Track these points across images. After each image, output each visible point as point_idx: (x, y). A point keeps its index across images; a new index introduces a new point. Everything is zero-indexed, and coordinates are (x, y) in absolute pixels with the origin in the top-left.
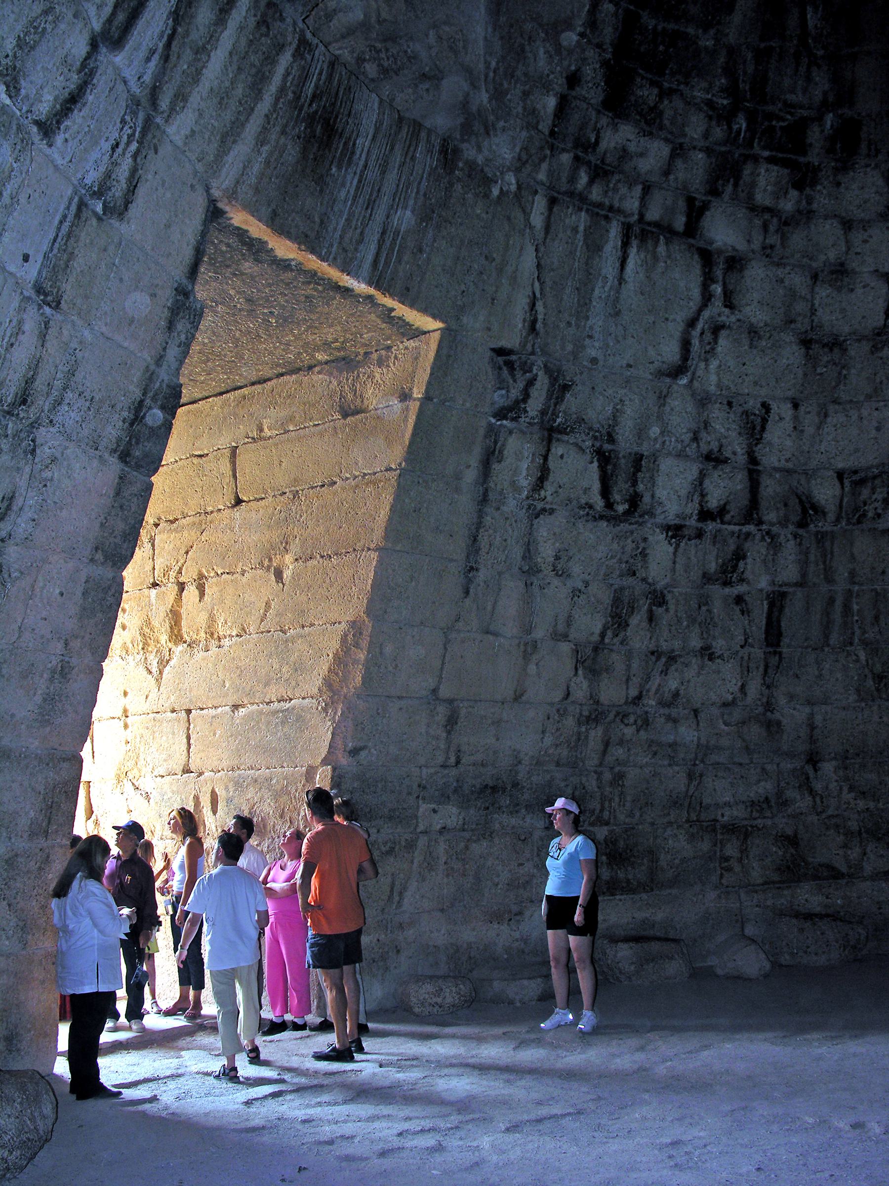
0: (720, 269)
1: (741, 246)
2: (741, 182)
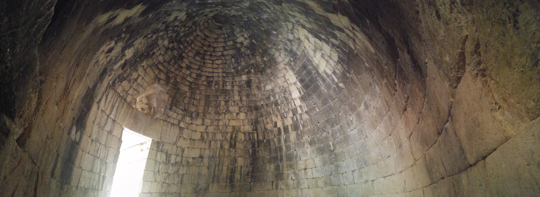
0: (181, 129)
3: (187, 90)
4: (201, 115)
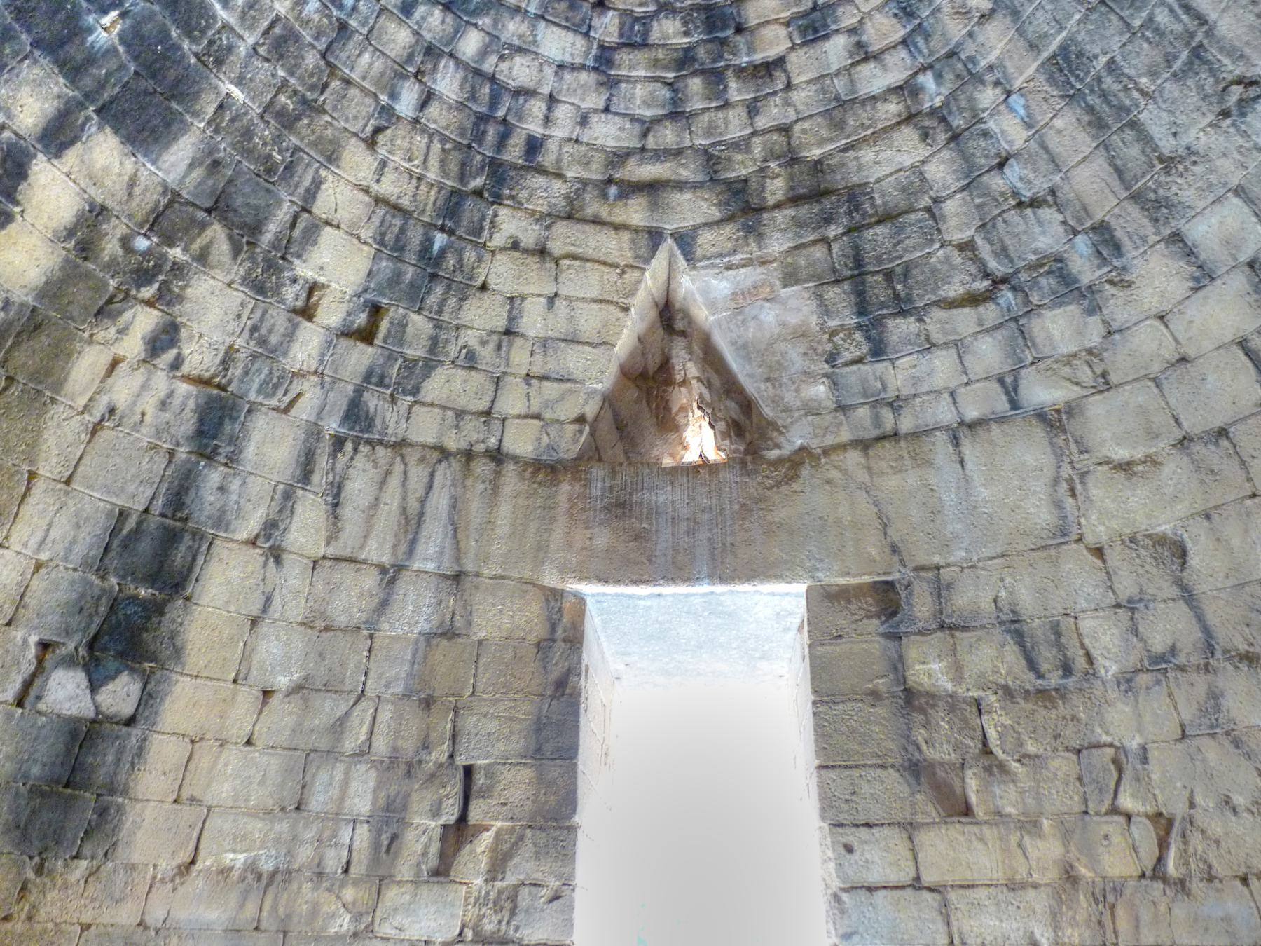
1: (1076, 391)
2: (1038, 340)
3: (923, 151)
4: (1129, 221)
